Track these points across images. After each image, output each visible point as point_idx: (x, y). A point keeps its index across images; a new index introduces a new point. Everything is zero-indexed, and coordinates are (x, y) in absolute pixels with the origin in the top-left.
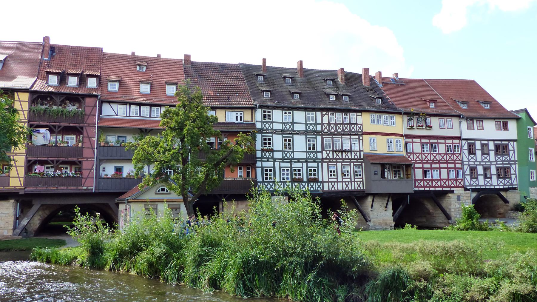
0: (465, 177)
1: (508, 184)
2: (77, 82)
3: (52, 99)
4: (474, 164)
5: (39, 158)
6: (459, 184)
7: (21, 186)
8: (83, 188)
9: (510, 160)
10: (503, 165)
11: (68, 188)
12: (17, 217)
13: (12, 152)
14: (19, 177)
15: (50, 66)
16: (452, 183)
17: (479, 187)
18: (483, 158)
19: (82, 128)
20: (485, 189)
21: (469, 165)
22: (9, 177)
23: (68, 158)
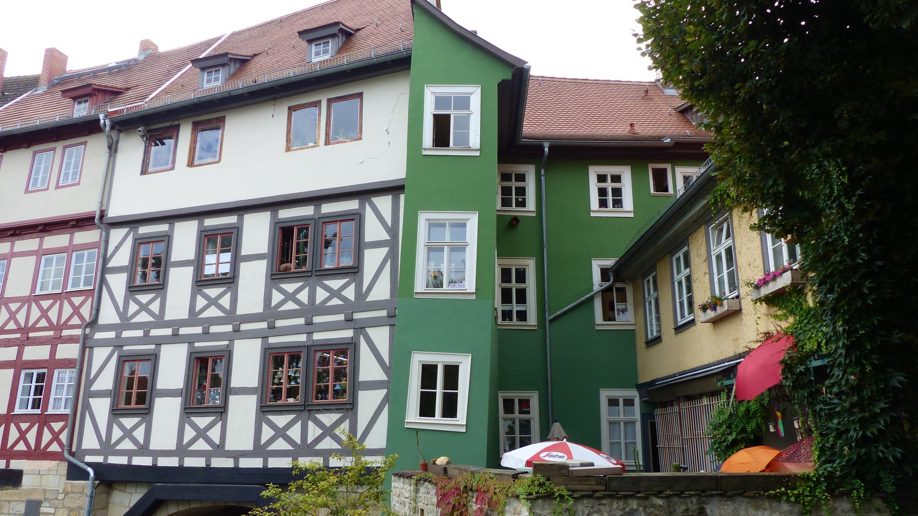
0: (87, 407)
1: (328, 443)
4: (146, 338)
6: (49, 444)
9: (361, 301)
10: (310, 334)
16: (23, 436)
17: (146, 461)
18: (201, 302)
20: (181, 469)
21: (117, 344)
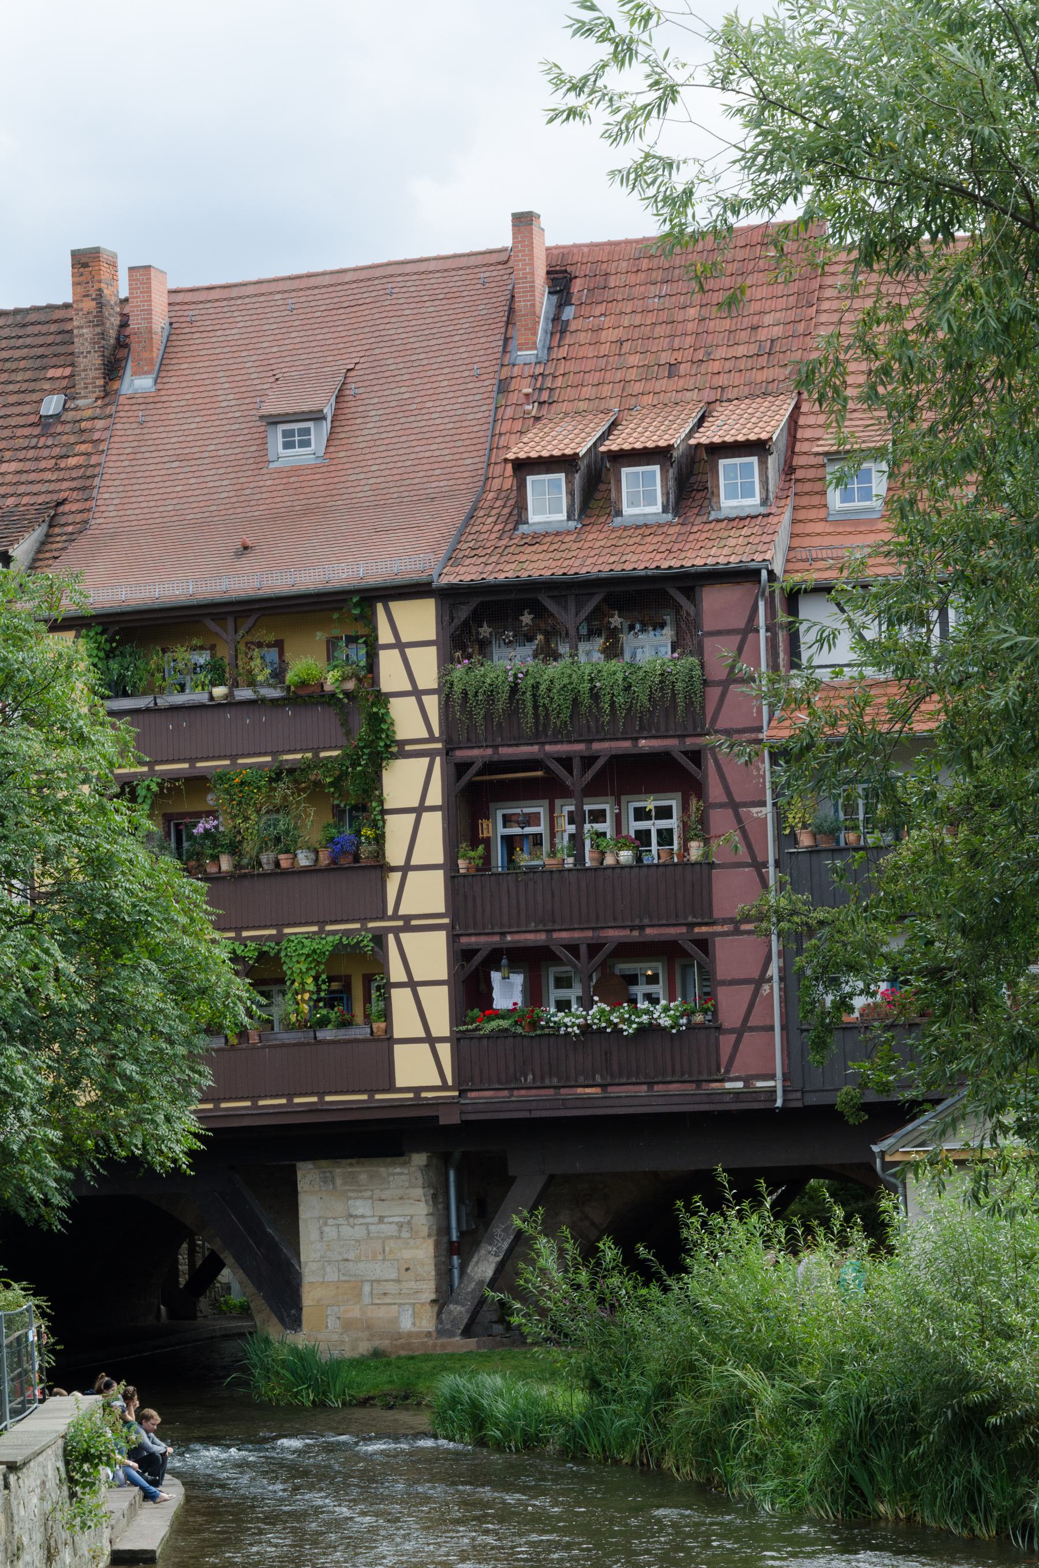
2: (666, 494)
3: (540, 611)
5: (509, 938)
7: (444, 1087)
8: (728, 1085)
11: (656, 1088)
12: (451, 1243)
13: (390, 912)
14: (431, 1040)
15: (545, 396)
19: (696, 756)
22: (389, 1041)
23: (642, 928)
